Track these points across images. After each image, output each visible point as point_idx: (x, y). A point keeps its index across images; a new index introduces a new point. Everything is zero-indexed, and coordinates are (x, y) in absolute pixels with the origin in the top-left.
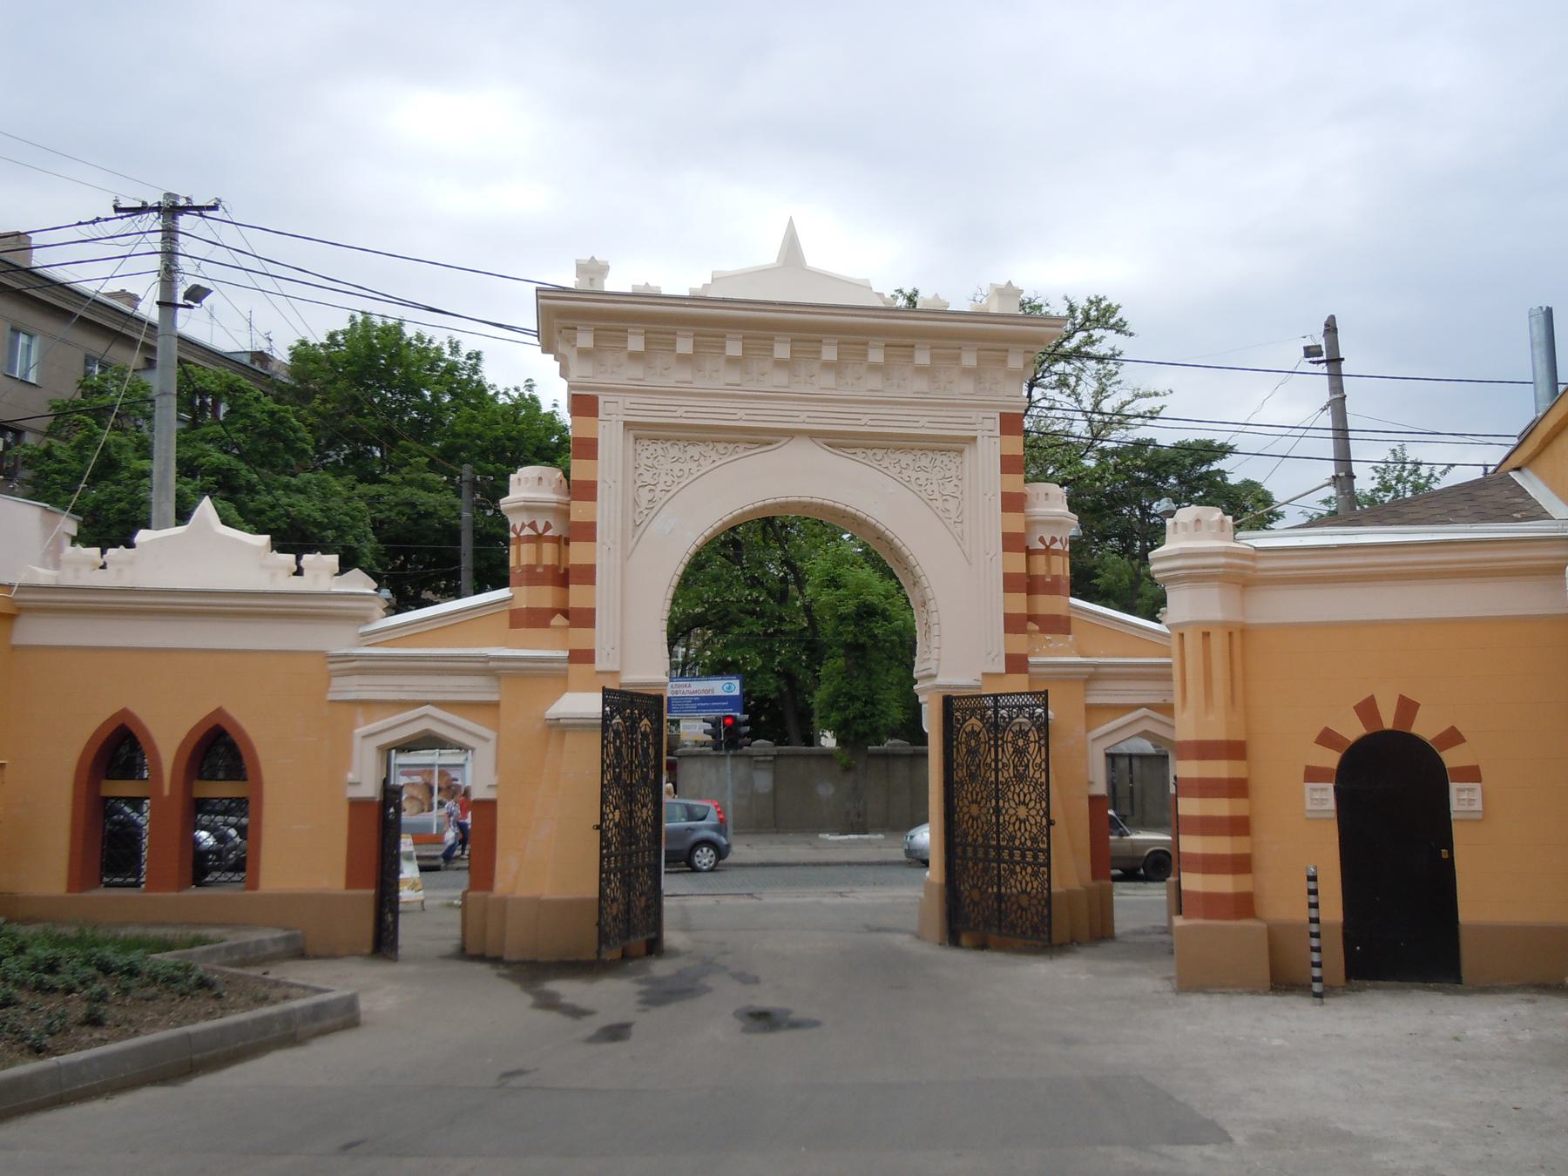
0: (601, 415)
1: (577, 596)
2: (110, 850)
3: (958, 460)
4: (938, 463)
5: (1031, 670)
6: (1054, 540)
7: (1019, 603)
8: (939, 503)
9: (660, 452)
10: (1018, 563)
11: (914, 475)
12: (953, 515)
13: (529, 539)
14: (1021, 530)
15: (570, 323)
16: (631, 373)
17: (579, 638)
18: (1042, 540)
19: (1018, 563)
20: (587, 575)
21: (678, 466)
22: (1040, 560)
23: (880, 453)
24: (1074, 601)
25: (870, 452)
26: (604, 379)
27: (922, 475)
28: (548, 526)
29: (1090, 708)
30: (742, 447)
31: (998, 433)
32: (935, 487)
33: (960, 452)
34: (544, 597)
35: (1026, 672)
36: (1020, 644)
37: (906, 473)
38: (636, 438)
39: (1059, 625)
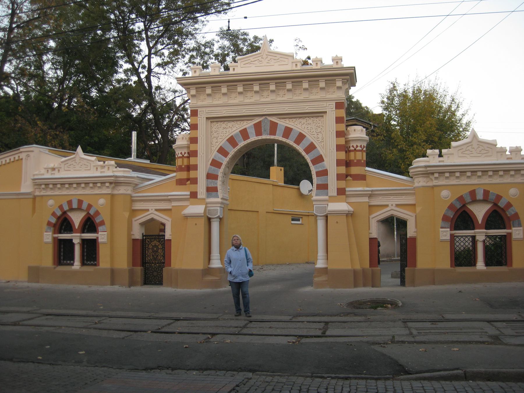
1: (192, 174)
2: (63, 252)
3: (322, 120)
4: (315, 121)
5: (347, 193)
6: (357, 146)
7: (343, 170)
8: (316, 136)
9: (219, 126)
10: (342, 155)
11: (306, 126)
12: (320, 140)
13: (180, 157)
14: (344, 143)
16: (208, 101)
17: (192, 188)
18: (353, 146)
19: (342, 155)
20: (195, 167)
21: (225, 130)
22: (352, 154)
23: (294, 120)
24: (367, 169)
26: (200, 103)
27: (309, 126)
28: (185, 153)
29: (370, 206)
30: (245, 122)
31: (334, 109)
32: (314, 130)
33: (323, 116)
34: (183, 175)
36: (342, 184)
37: (303, 126)
38: (211, 122)
39: (362, 178)
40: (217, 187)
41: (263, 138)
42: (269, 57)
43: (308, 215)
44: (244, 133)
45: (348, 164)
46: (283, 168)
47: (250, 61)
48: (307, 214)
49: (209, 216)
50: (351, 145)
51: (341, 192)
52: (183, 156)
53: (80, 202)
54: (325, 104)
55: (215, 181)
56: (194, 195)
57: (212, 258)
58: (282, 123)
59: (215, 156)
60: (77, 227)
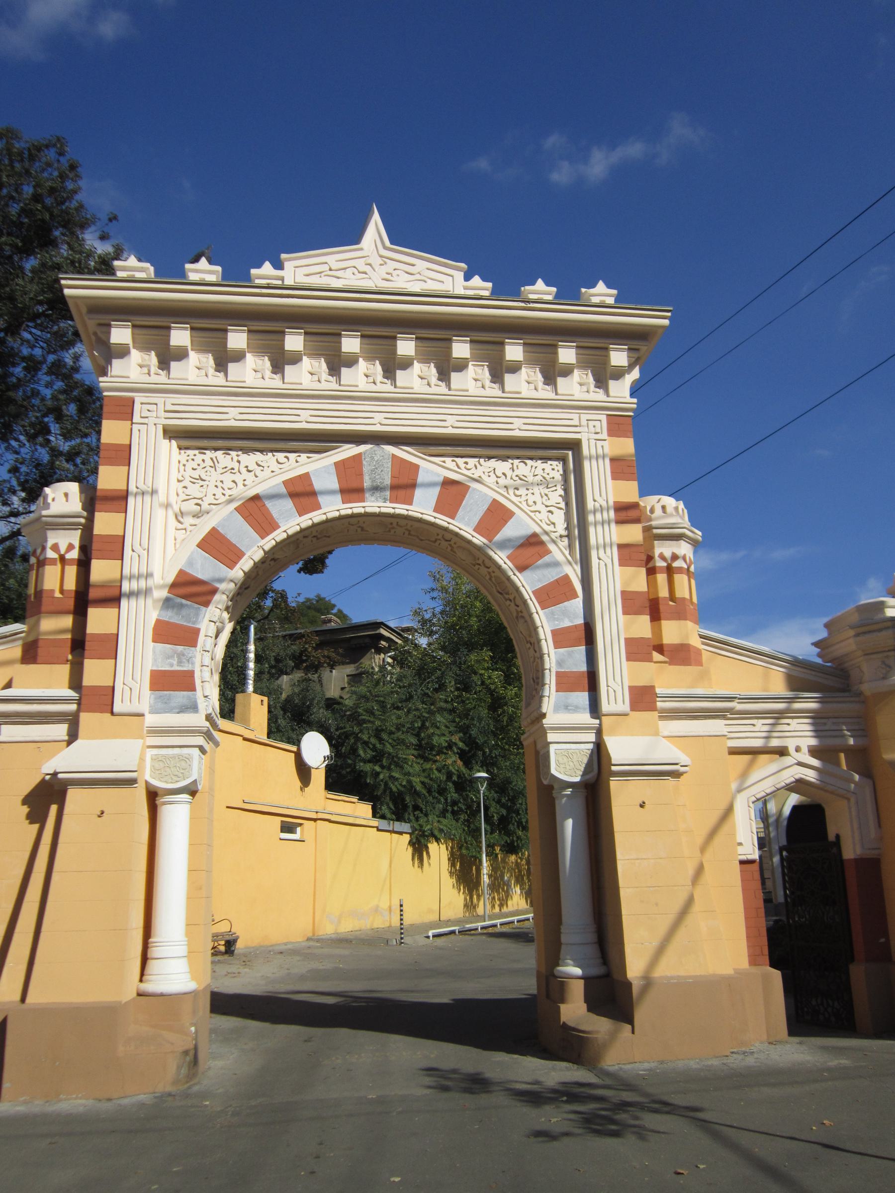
0: (136, 418)
7: (642, 626)
8: (544, 515)
10: (639, 581)
15: (103, 319)
19: (639, 581)
21: (228, 478)
25: (461, 461)
28: (71, 547)
31: (604, 435)
35: (653, 708)
40: (191, 674)
42: (392, 265)
43: (315, 820)
44: (302, 493)
45: (655, 610)
47: (326, 267)
48: (314, 816)
51: (643, 698)
52: (62, 558)
55: (188, 651)
57: (153, 952)
58: (433, 469)
59: (190, 562)
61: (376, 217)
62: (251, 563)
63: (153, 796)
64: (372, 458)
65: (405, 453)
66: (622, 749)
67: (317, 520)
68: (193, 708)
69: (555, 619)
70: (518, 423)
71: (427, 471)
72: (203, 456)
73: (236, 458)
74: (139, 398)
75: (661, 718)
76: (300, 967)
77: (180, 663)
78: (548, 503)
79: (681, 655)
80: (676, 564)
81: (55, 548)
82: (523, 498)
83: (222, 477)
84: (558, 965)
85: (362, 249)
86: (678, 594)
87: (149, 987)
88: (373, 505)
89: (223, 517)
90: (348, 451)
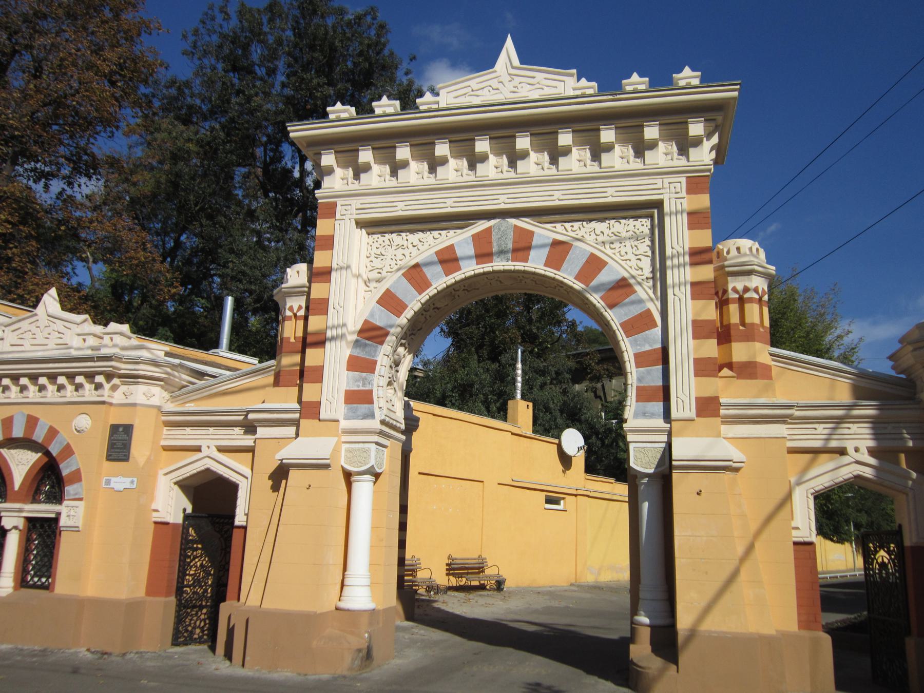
0: (338, 216)
5: (722, 412)
7: (710, 349)
8: (634, 263)
10: (710, 312)
15: (316, 149)
21: (400, 251)
25: (568, 225)
28: (300, 308)
30: (452, 232)
31: (684, 194)
35: (717, 415)
41: (495, 268)
43: (576, 495)
44: (448, 259)
45: (724, 335)
46: (531, 404)
48: (574, 492)
49: (349, 467)
50: (730, 287)
51: (708, 407)
52: (295, 315)
53: (32, 422)
54: (658, 182)
56: (311, 410)
57: (347, 582)
58: (544, 233)
59: (372, 314)
60: (17, 486)
61: (509, 43)
62: (412, 313)
63: (348, 476)
64: (499, 229)
65: (524, 224)
66: (682, 450)
67: (458, 279)
68: (372, 416)
69: (637, 345)
70: (611, 191)
71: (540, 235)
72: (383, 238)
73: (405, 238)
74: (340, 202)
75: (723, 423)
76: (541, 603)
77: (364, 385)
78: (637, 253)
79: (748, 370)
80: (747, 296)
81: (291, 309)
82: (617, 250)
83: (395, 252)
84: (636, 615)
85: (495, 71)
86: (748, 320)
87: (342, 605)
88: (499, 264)
89: (394, 281)
90: (481, 226)
